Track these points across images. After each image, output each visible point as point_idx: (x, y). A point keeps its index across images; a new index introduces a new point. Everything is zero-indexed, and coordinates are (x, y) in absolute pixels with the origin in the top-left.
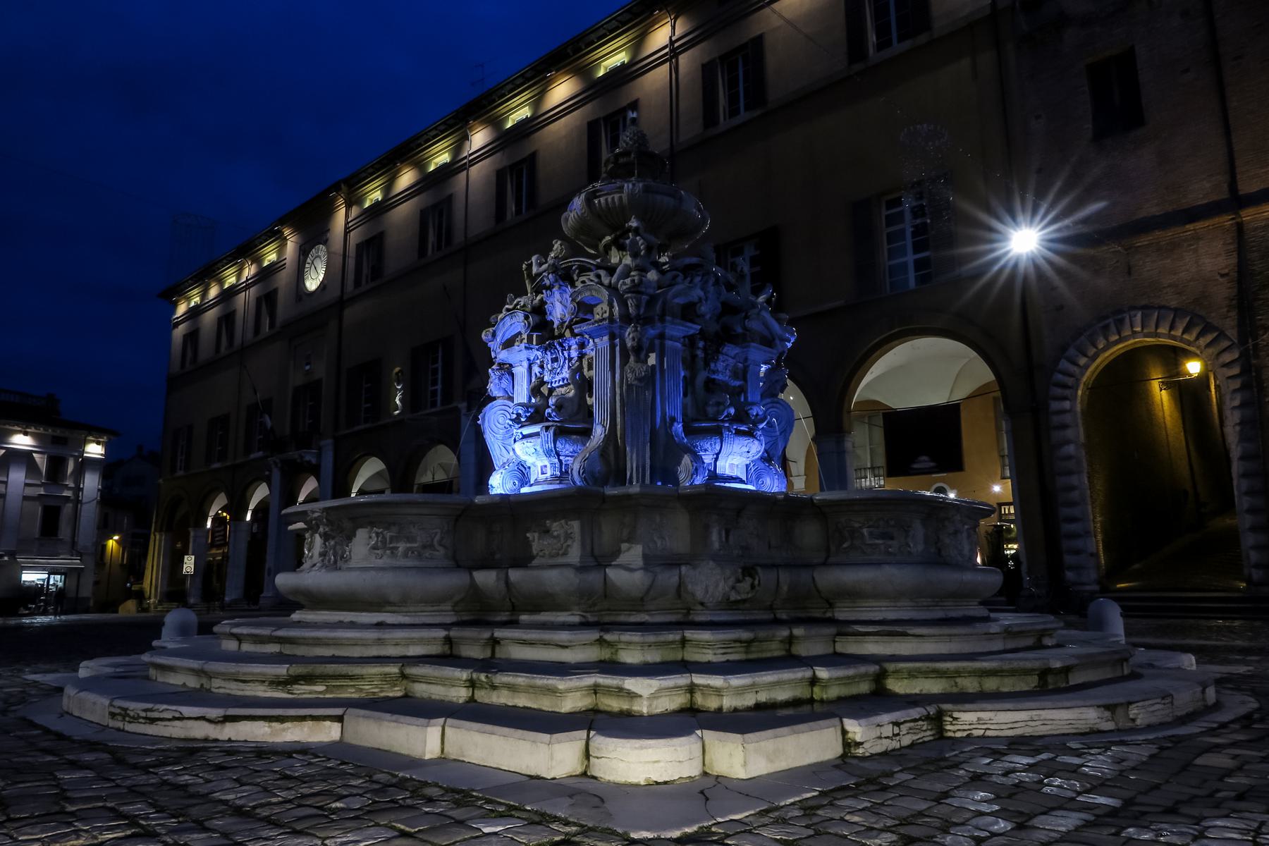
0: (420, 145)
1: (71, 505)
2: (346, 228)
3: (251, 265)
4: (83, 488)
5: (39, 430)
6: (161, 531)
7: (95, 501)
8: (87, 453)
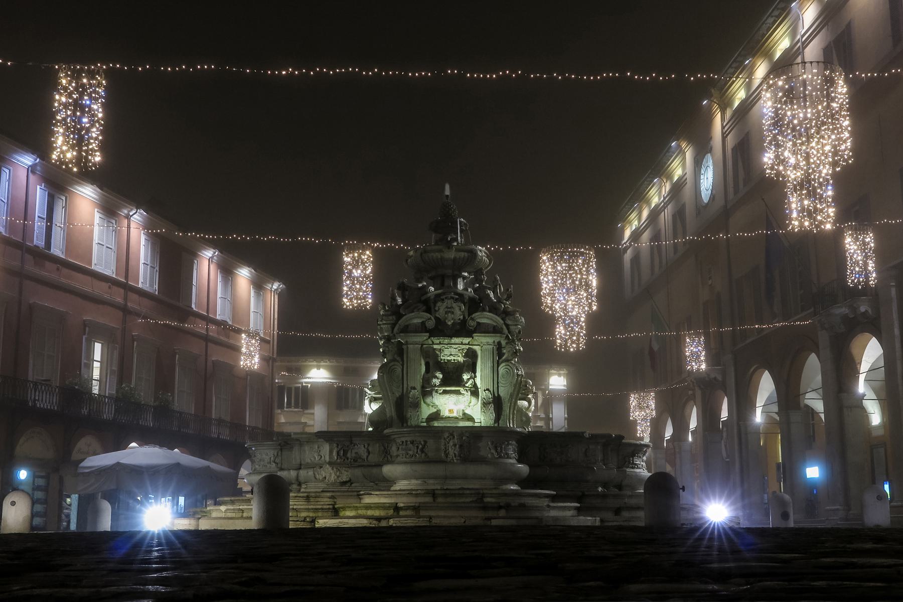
0: (764, 35)
2: (723, 134)
3: (666, 182)
4: (552, 418)
8: (551, 385)
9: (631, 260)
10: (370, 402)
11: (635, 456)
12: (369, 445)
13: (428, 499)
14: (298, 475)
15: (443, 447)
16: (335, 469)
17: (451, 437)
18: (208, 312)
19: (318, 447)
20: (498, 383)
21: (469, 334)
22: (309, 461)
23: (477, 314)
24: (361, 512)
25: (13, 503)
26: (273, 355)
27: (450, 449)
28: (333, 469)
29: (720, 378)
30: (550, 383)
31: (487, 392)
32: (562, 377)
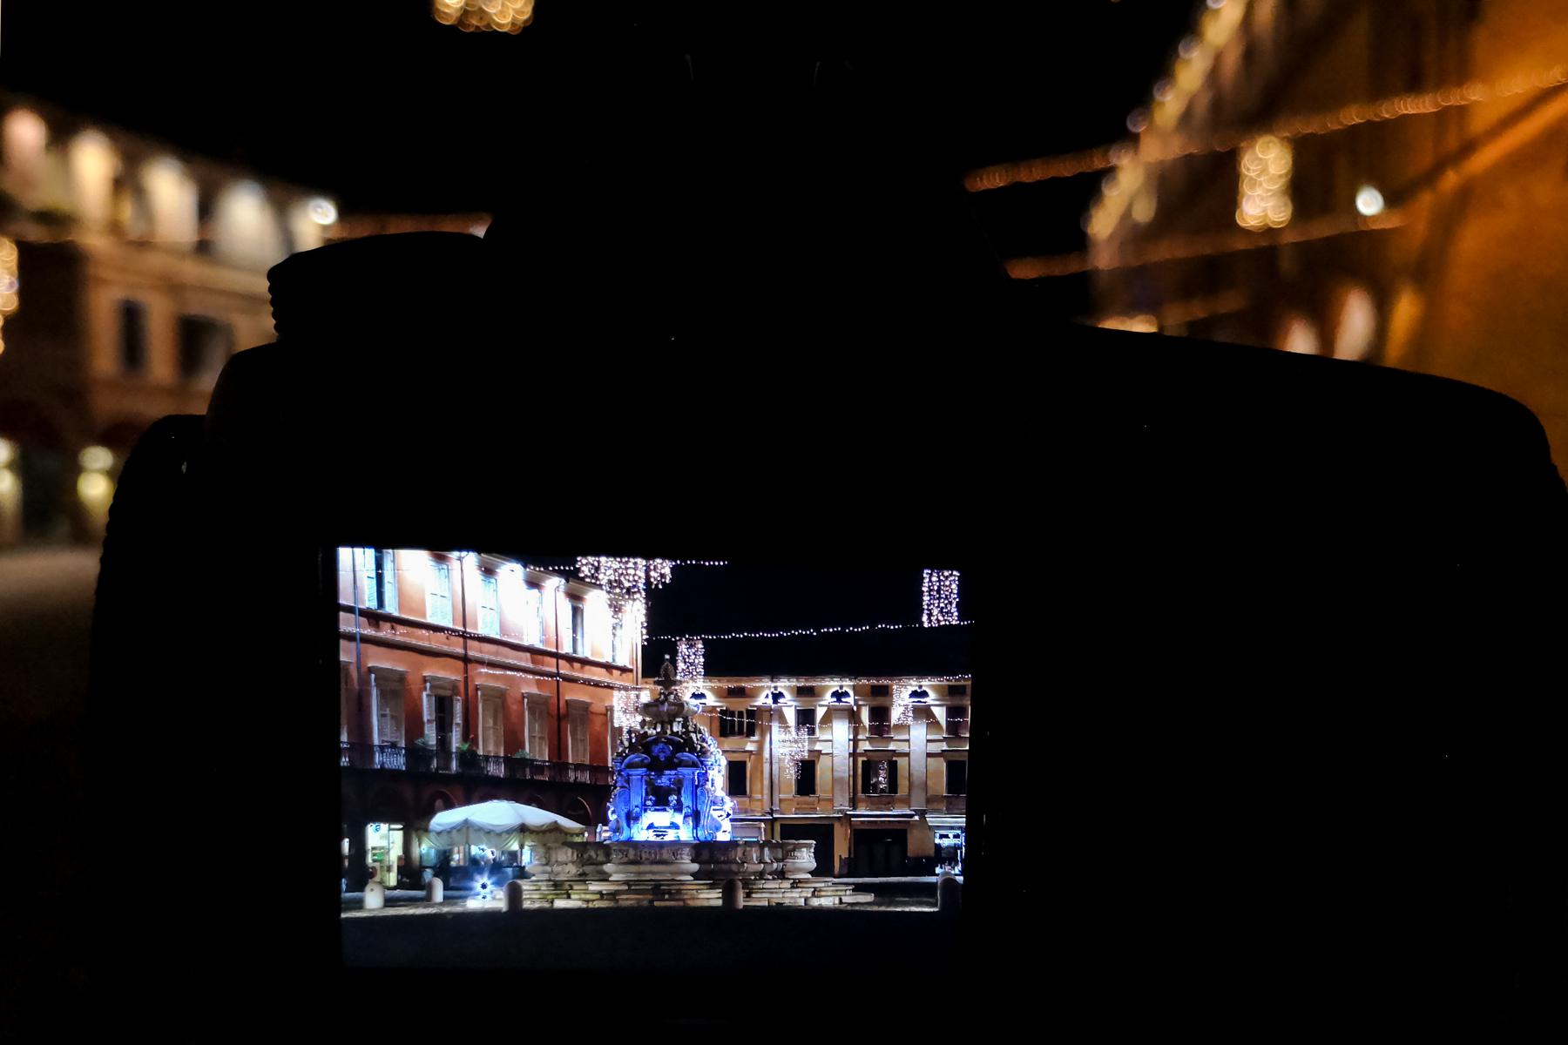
13: (627, 888)
18: (557, 648)
21: (673, 766)
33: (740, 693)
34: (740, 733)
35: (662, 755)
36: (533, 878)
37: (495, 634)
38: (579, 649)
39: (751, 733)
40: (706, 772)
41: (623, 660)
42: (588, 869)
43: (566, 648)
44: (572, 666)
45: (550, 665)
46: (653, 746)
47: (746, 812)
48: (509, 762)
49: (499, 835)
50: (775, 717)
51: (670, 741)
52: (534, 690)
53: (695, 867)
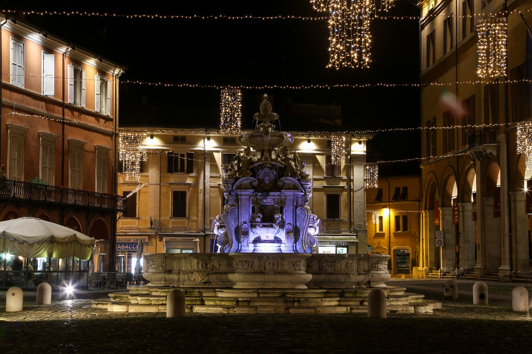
1: (346, 193)
5: (324, 137)
6: (426, 209)
7: (363, 189)
8: (352, 151)
9: (428, 36)
10: (218, 228)
11: (379, 263)
12: (220, 261)
13: (255, 295)
14: (179, 277)
15: (263, 265)
16: (201, 275)
17: (268, 259)
18: (63, 99)
19: (190, 261)
20: (296, 219)
21: (279, 189)
22: (185, 269)
23: (284, 178)
24: (218, 303)
25: (13, 294)
26: (116, 131)
27: (267, 266)
28: (199, 275)
29: (495, 153)
30: (352, 149)
31: (289, 225)
32: (362, 144)
33: (182, 140)
34: (182, 170)
35: (267, 178)
36: (149, 284)
37: (21, 85)
38: (78, 101)
39: (190, 171)
40: (305, 194)
41: (106, 111)
42: (213, 277)
43: (70, 100)
44: (73, 115)
45: (58, 112)
46: (260, 171)
47: (185, 230)
48: (29, 187)
49: (32, 245)
50: (208, 159)
51: (273, 167)
52: (47, 131)
53: (310, 277)
